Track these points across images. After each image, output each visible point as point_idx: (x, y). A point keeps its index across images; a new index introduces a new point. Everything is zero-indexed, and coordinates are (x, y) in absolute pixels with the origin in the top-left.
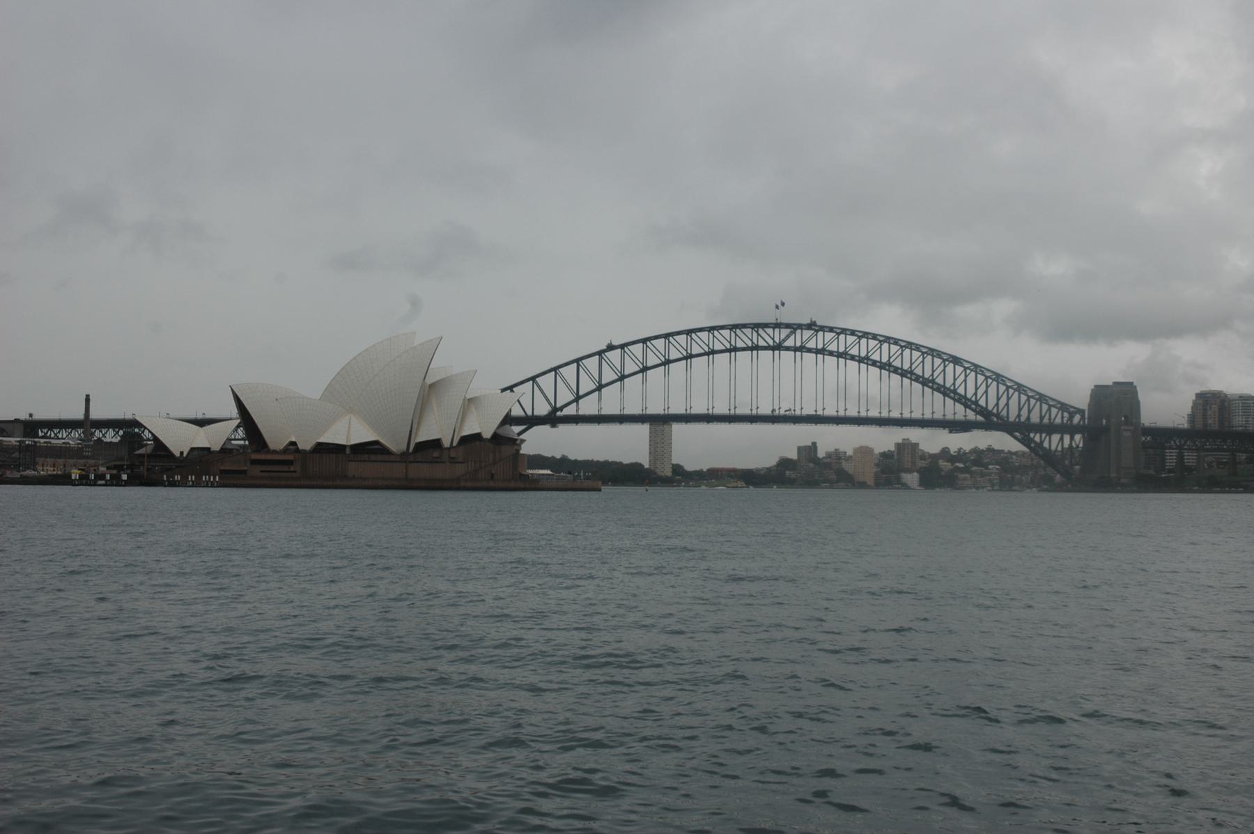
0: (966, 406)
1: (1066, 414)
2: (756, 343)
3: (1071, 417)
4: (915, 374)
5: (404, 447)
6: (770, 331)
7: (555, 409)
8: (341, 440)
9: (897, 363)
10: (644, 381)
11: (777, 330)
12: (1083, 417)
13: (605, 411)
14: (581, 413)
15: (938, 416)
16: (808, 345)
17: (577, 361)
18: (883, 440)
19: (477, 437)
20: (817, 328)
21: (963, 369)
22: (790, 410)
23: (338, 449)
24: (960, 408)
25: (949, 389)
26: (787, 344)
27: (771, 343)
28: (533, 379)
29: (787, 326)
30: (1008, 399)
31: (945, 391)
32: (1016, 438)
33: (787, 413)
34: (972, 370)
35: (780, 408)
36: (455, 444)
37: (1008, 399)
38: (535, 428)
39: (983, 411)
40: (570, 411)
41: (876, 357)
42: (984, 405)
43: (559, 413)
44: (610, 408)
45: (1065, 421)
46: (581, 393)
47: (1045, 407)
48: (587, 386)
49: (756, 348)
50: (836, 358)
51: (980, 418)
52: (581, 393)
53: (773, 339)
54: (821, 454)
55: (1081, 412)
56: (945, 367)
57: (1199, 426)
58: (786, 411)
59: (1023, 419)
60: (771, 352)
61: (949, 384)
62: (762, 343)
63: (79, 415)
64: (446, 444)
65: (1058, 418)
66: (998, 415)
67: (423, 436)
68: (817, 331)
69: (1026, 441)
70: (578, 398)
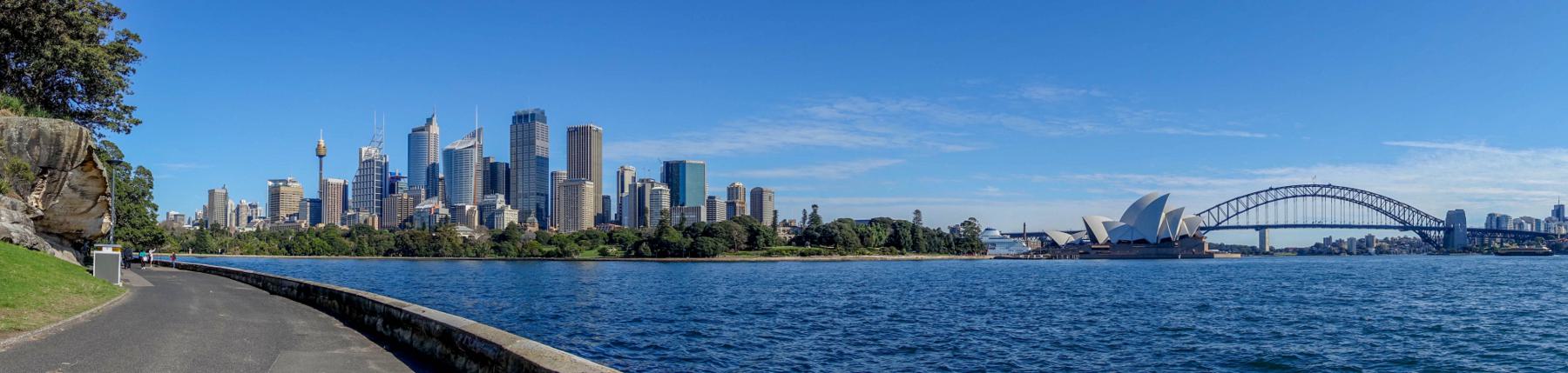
3: (1439, 223)
7: (1219, 223)
9: (1366, 202)
10: (1257, 210)
13: (1241, 224)
14: (1230, 225)
15: (1383, 224)
17: (1228, 202)
28: (1209, 210)
29: (1319, 186)
31: (1386, 213)
39: (1403, 222)
40: (1225, 224)
41: (1357, 199)
48: (1232, 213)
49: (1306, 195)
51: (1401, 225)
55: (1442, 221)
57: (1489, 227)
61: (1388, 210)
69: (1419, 234)
70: (1228, 219)
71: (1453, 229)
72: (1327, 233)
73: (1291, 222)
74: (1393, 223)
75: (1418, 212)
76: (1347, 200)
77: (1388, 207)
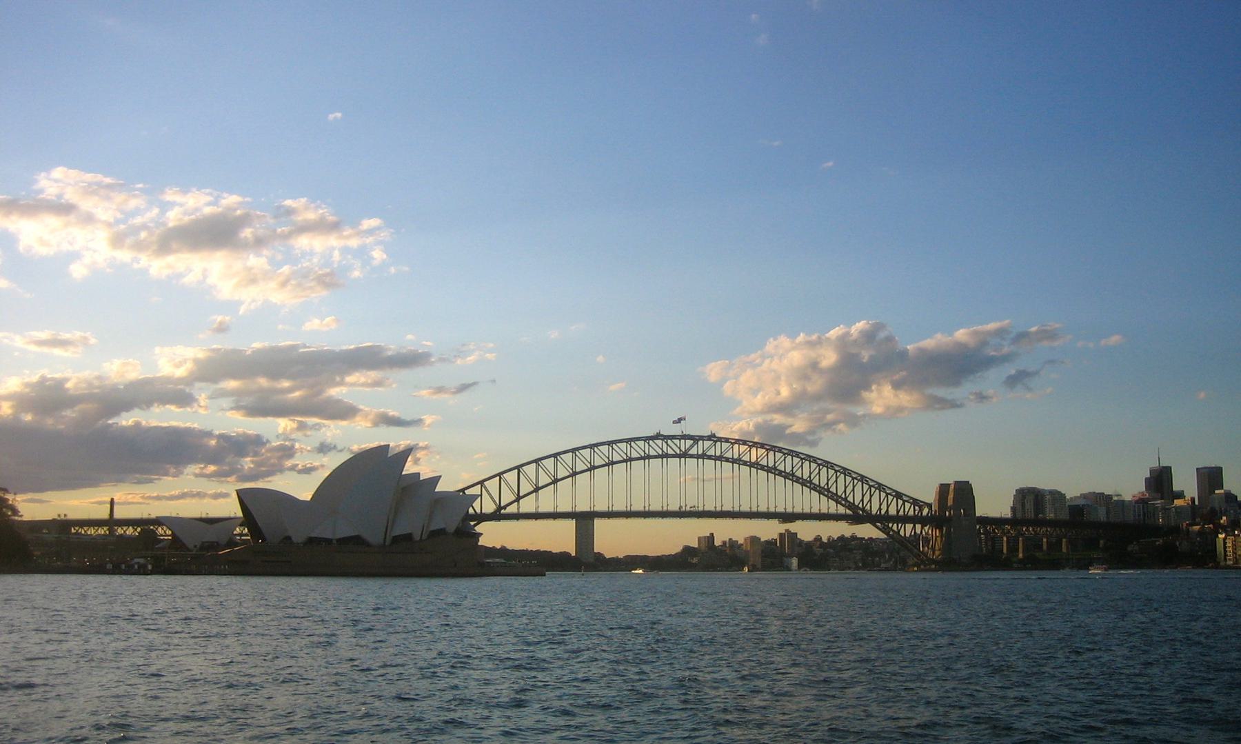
0: (837, 502)
1: (917, 508)
2: (666, 451)
3: (921, 510)
4: (796, 476)
5: (382, 541)
6: (677, 442)
7: (500, 508)
8: (328, 535)
9: (781, 468)
11: (683, 441)
12: (930, 508)
13: (541, 510)
14: (523, 510)
15: (815, 510)
16: (708, 453)
18: (769, 531)
19: (441, 532)
20: (715, 439)
21: (834, 471)
22: (694, 507)
23: (328, 541)
24: (832, 503)
25: (823, 488)
26: (690, 452)
27: (678, 452)
30: (871, 496)
32: (877, 527)
33: (692, 509)
34: (841, 473)
35: (686, 506)
36: (424, 537)
37: (871, 496)
38: (483, 523)
39: (851, 506)
40: (512, 509)
42: (852, 501)
43: (503, 511)
44: (546, 507)
45: (916, 512)
46: (521, 494)
47: (900, 502)
48: (526, 487)
49: (667, 456)
50: (731, 464)
51: (849, 512)
52: (521, 494)
53: (680, 448)
54: (718, 543)
55: (930, 506)
56: (820, 470)
57: (1019, 516)
58: (691, 508)
59: (883, 512)
60: (678, 459)
62: (670, 452)
63: (103, 514)
64: (417, 537)
65: (910, 510)
66: (863, 509)
67: (398, 531)
68: (715, 442)
69: (885, 530)
70: (518, 498)
71: (950, 518)
72: (704, 527)
73: (638, 506)
74: (833, 507)
75: (880, 487)
76: (745, 463)
77: (823, 478)
